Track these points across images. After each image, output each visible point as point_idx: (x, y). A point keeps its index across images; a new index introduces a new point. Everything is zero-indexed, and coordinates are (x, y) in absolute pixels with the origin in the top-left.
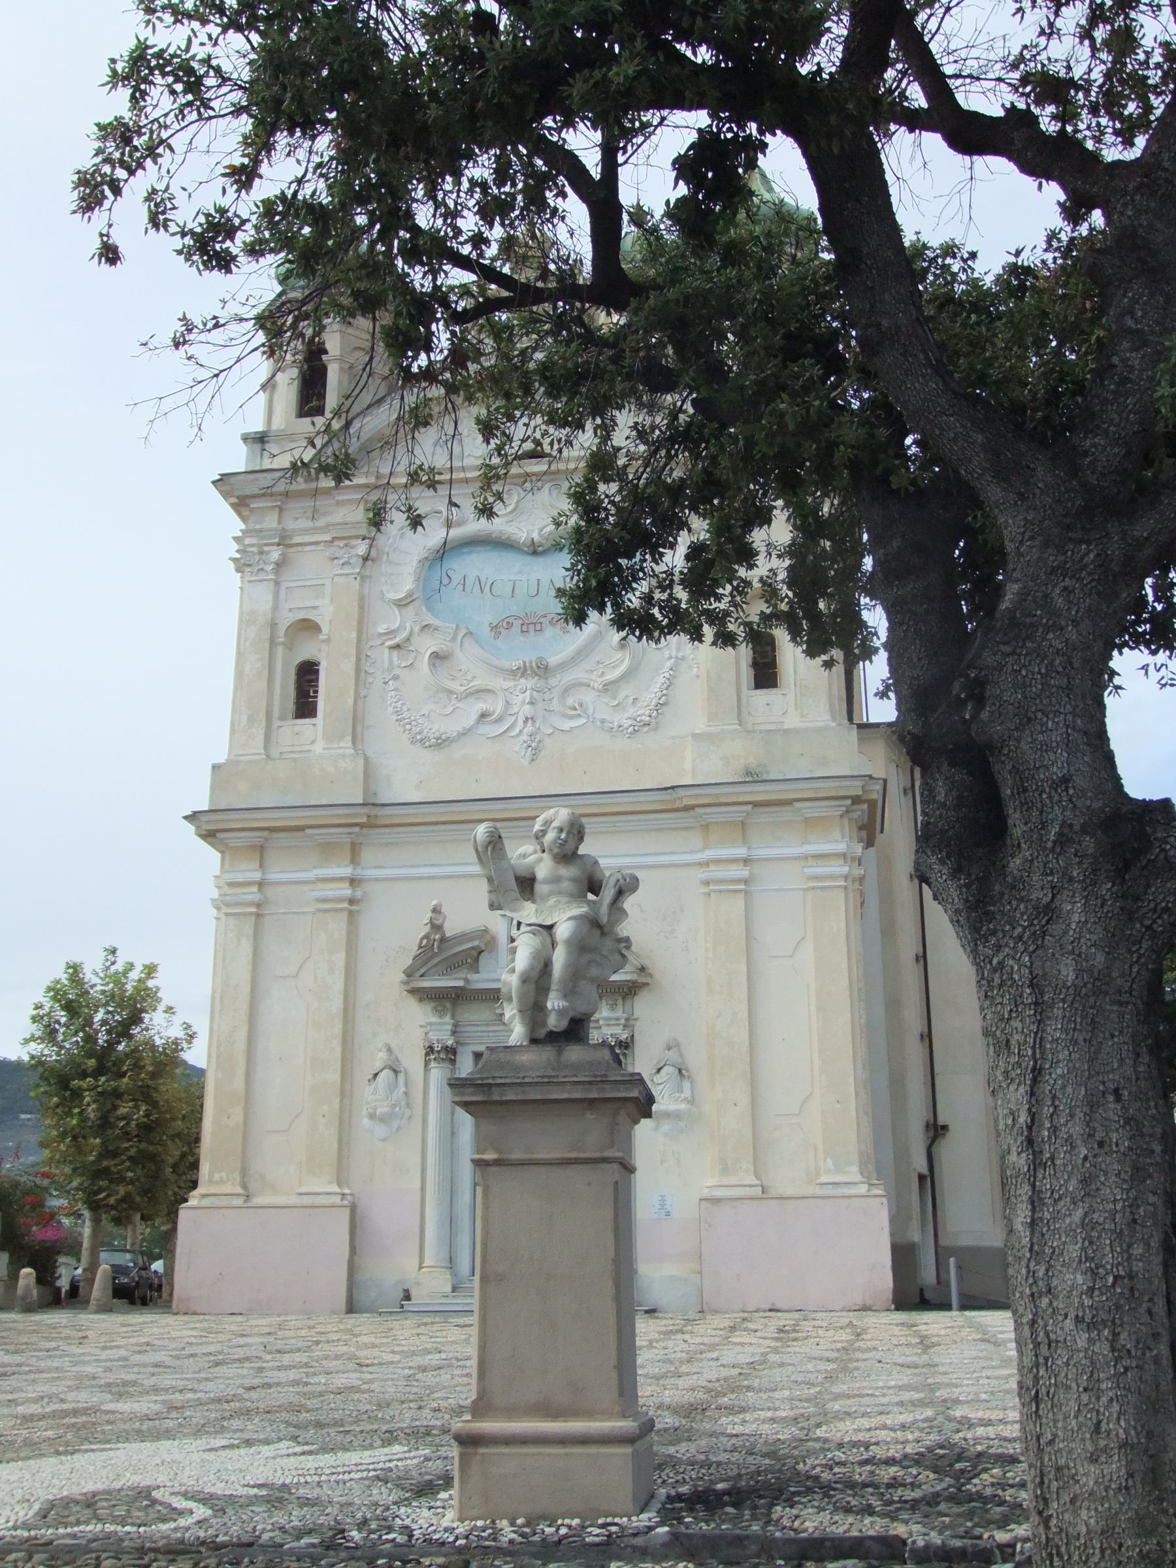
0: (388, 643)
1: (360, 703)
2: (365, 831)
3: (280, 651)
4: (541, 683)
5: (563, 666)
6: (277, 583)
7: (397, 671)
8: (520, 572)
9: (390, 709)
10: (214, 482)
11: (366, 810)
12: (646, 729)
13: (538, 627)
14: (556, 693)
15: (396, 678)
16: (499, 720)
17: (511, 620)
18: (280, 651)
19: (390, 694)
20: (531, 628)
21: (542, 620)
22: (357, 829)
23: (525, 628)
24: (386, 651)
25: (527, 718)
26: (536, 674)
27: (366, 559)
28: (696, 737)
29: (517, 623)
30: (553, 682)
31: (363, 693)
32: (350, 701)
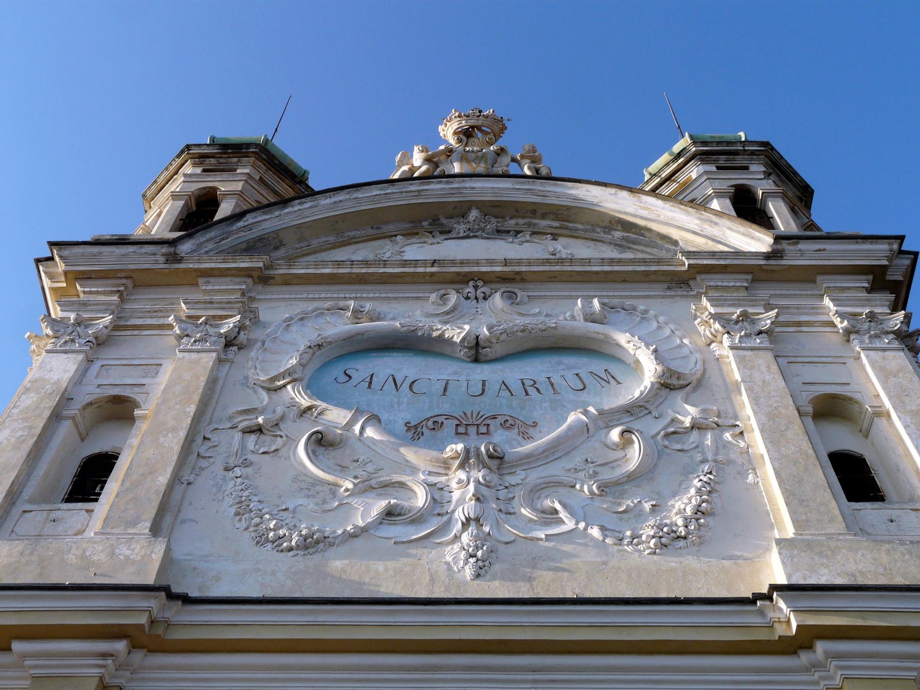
0: (242, 425)
1: (179, 489)
2: (138, 657)
3: (65, 428)
4: (494, 478)
5: (529, 460)
6: (90, 361)
7: (252, 457)
8: (455, 373)
9: (230, 500)
10: (38, 261)
11: (154, 603)
12: (682, 543)
13: (483, 429)
14: (519, 493)
15: (246, 464)
16: (418, 519)
17: (440, 420)
18: (65, 428)
19: (231, 484)
20: (472, 430)
21: (489, 422)
22: (120, 646)
23: (461, 430)
24: (238, 436)
25: (468, 520)
26: (485, 466)
27: (230, 342)
28: (779, 542)
29: (450, 425)
30: (511, 480)
31: (187, 476)
32: (163, 479)
